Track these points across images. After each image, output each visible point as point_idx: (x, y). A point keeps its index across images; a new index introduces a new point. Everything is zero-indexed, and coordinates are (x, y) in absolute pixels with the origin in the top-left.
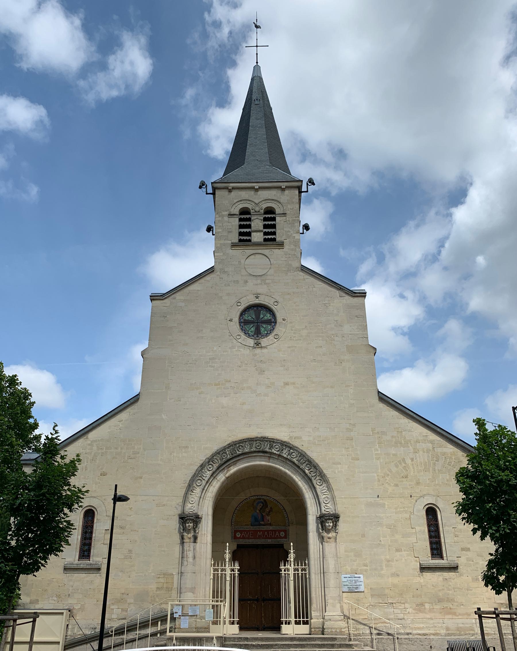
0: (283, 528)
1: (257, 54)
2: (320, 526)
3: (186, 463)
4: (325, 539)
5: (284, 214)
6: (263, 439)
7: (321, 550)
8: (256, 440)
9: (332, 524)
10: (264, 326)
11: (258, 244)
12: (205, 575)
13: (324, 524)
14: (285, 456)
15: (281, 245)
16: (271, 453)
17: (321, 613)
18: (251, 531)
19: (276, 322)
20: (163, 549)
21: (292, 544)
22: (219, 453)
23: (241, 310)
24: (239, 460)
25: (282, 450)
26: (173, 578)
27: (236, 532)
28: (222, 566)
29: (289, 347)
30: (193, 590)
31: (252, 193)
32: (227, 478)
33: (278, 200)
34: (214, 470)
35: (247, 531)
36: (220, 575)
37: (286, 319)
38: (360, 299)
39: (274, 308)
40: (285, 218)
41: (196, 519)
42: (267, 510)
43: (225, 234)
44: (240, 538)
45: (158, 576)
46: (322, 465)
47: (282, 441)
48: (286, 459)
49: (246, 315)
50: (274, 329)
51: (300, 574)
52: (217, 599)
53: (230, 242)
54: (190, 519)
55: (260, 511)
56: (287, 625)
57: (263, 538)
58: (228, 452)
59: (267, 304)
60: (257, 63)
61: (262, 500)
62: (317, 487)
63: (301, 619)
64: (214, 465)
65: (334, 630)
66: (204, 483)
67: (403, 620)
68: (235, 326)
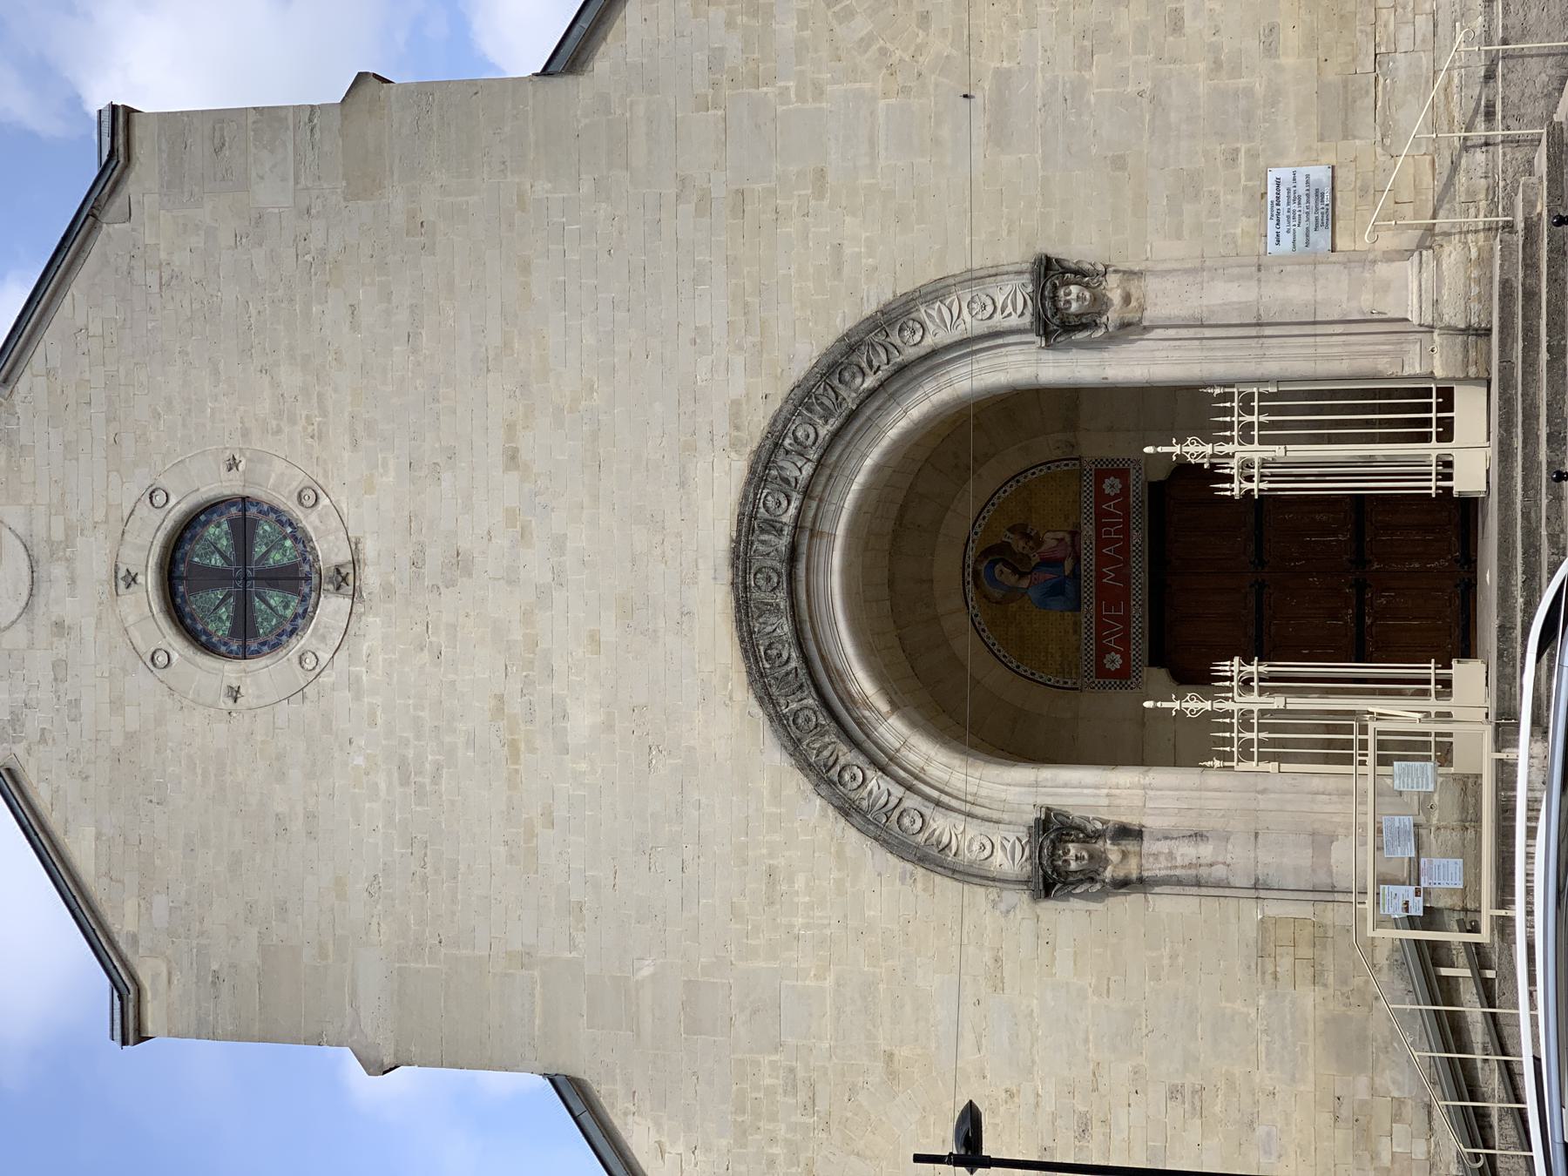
0: (1088, 484)
2: (1080, 336)
3: (835, 874)
4: (1130, 316)
6: (742, 558)
7: (1172, 333)
8: (746, 588)
9: (1074, 289)
10: (260, 550)
12: (1264, 791)
13: (1074, 321)
14: (808, 469)
16: (797, 526)
17: (1412, 337)
18: (1098, 606)
19: (244, 499)
20: (1166, 961)
21: (1148, 450)
22: (796, 743)
23: (190, 652)
24: (823, 658)
25: (786, 481)
26: (1276, 920)
27: (1102, 672)
28: (1230, 727)
29: (355, 444)
30: (1321, 841)
32: (895, 706)
34: (861, 760)
35: (1101, 626)
36: (1263, 735)
37: (228, 454)
38: (138, 132)
39: (179, 507)
41: (1053, 830)
42: (1019, 545)
44: (1125, 656)
45: (1269, 978)
46: (843, 319)
47: (748, 483)
48: (820, 464)
49: (211, 627)
50: (273, 509)
51: (1263, 418)
52: (1356, 745)
54: (1052, 854)
55: (1022, 575)
56: (1456, 472)
57: (1127, 563)
58: (794, 706)
59: (161, 537)
61: (982, 568)
62: (929, 341)
63: (1433, 415)
64: (842, 761)
65: (1475, 290)
66: (912, 802)
67: (1440, 17)
68: (261, 676)
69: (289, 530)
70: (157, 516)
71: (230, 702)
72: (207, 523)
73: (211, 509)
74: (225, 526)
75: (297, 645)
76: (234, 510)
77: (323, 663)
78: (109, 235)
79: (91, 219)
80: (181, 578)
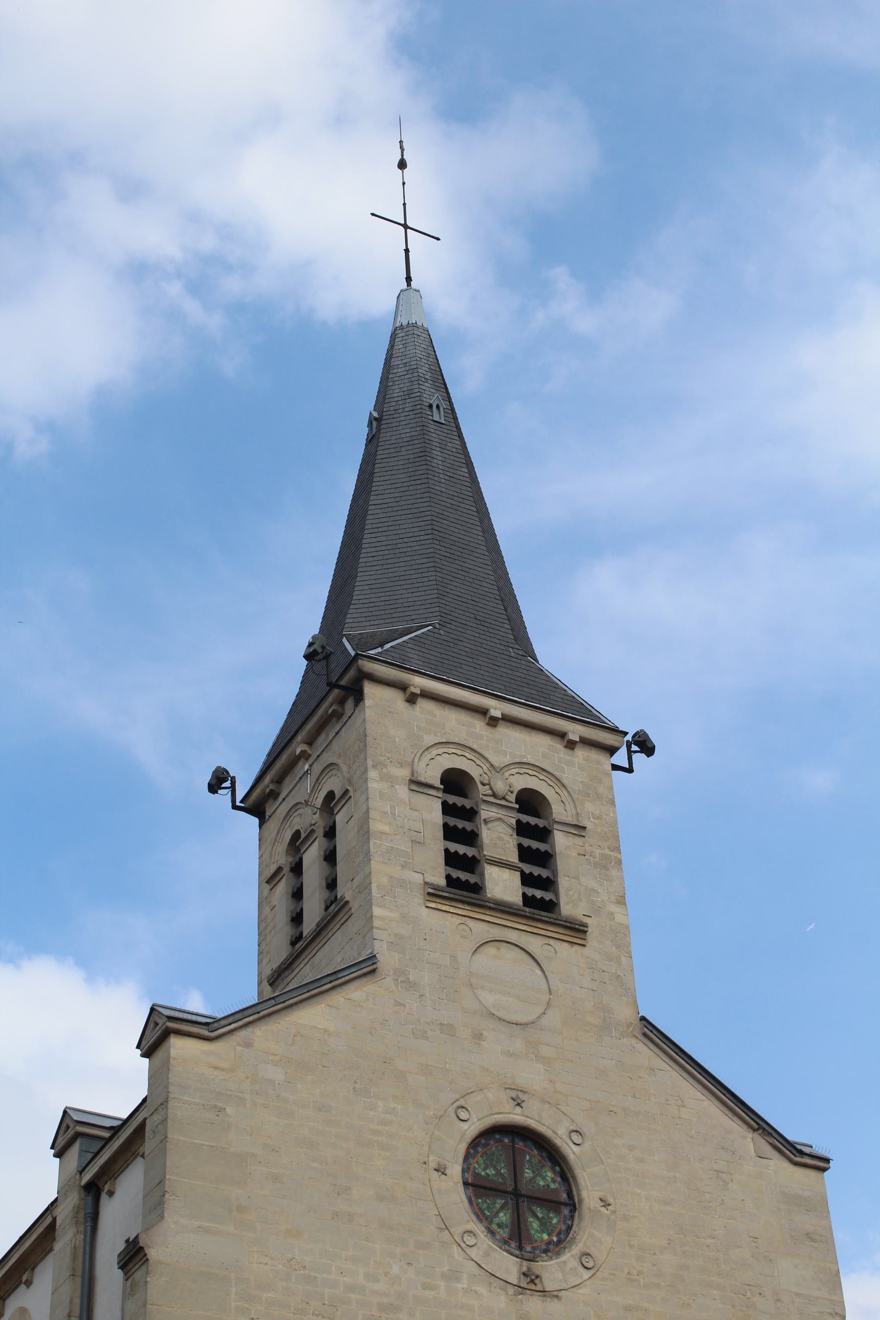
1: (407, 251)
5: (579, 829)
11: (502, 908)
15: (576, 930)
31: (478, 725)
33: (556, 773)
37: (611, 1200)
38: (812, 1174)
39: (571, 1151)
40: (579, 841)
43: (405, 847)
53: (418, 878)
59: (548, 1133)
60: (409, 279)
69: (555, 1239)
70: (562, 1131)
71: (433, 1165)
72: (554, 1172)
73: (565, 1174)
74: (553, 1186)
75: (479, 1229)
76: (565, 1195)
77: (468, 1250)
78: (745, 1138)
79: (756, 1126)
80: (513, 1141)
